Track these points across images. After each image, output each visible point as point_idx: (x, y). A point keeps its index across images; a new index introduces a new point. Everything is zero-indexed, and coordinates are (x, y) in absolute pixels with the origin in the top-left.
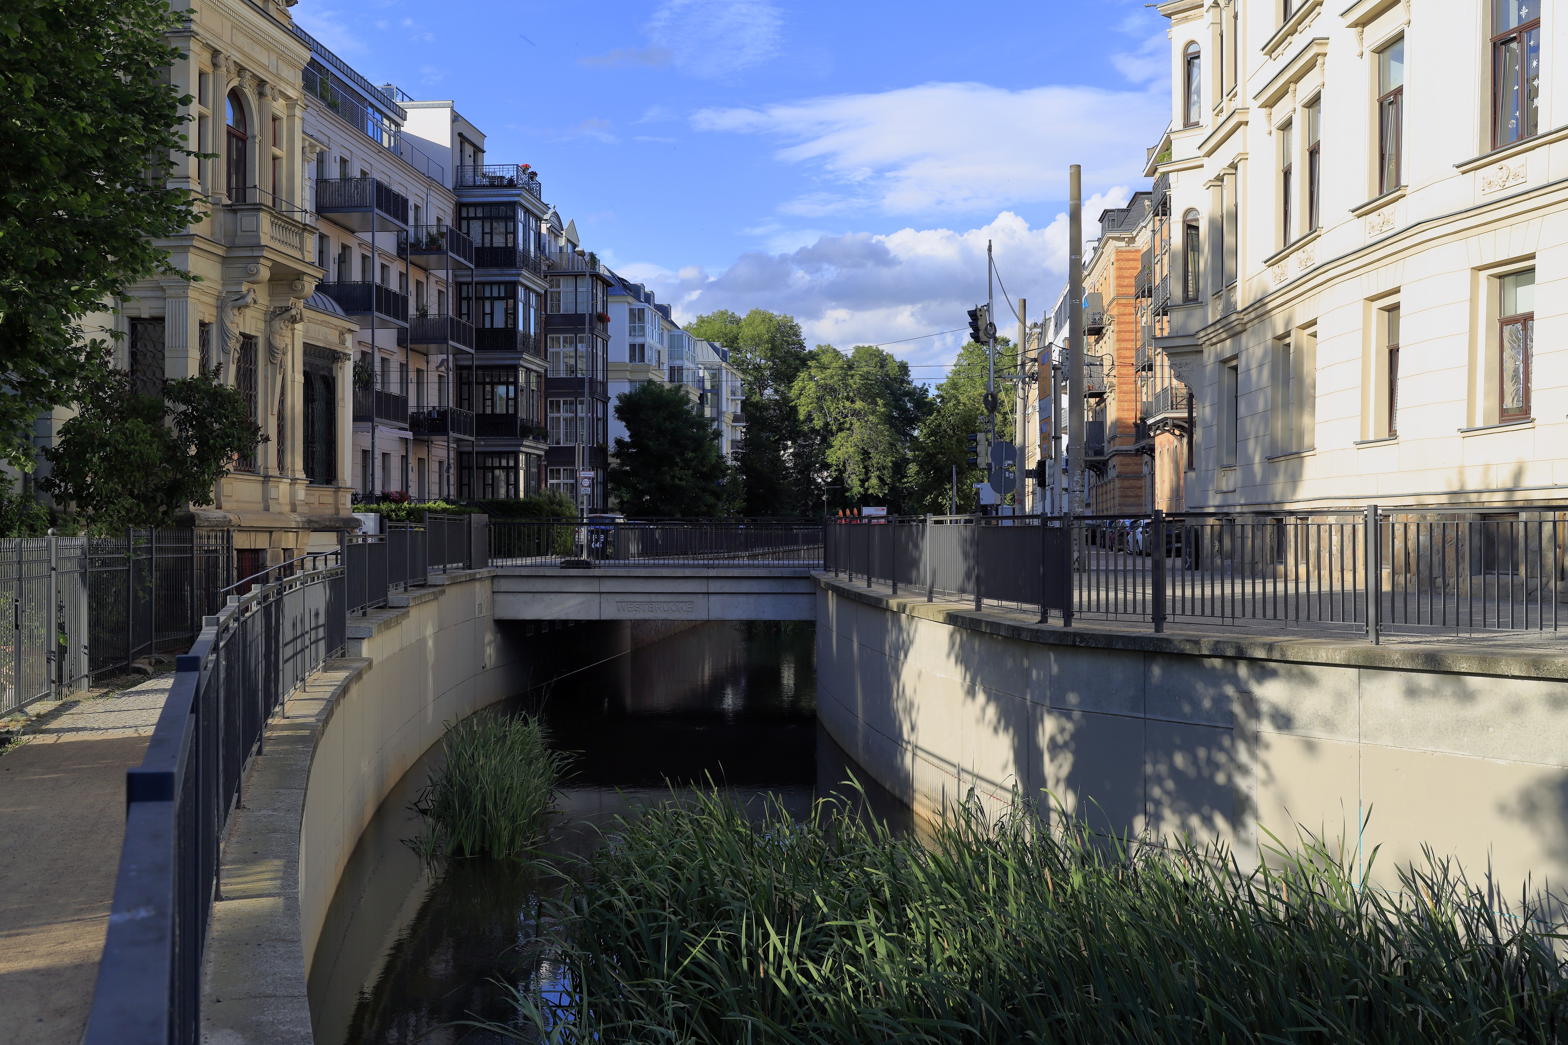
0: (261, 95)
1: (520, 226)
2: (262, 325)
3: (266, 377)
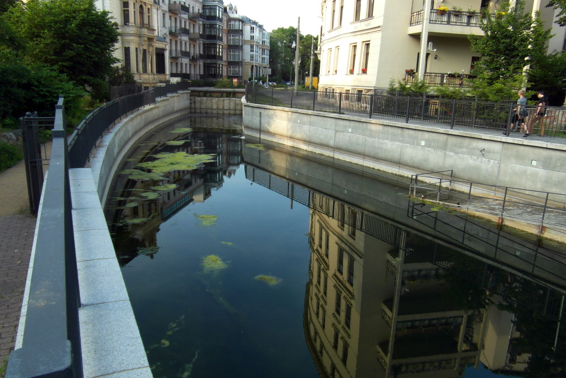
0: (146, 5)
1: (217, 11)
2: (147, 47)
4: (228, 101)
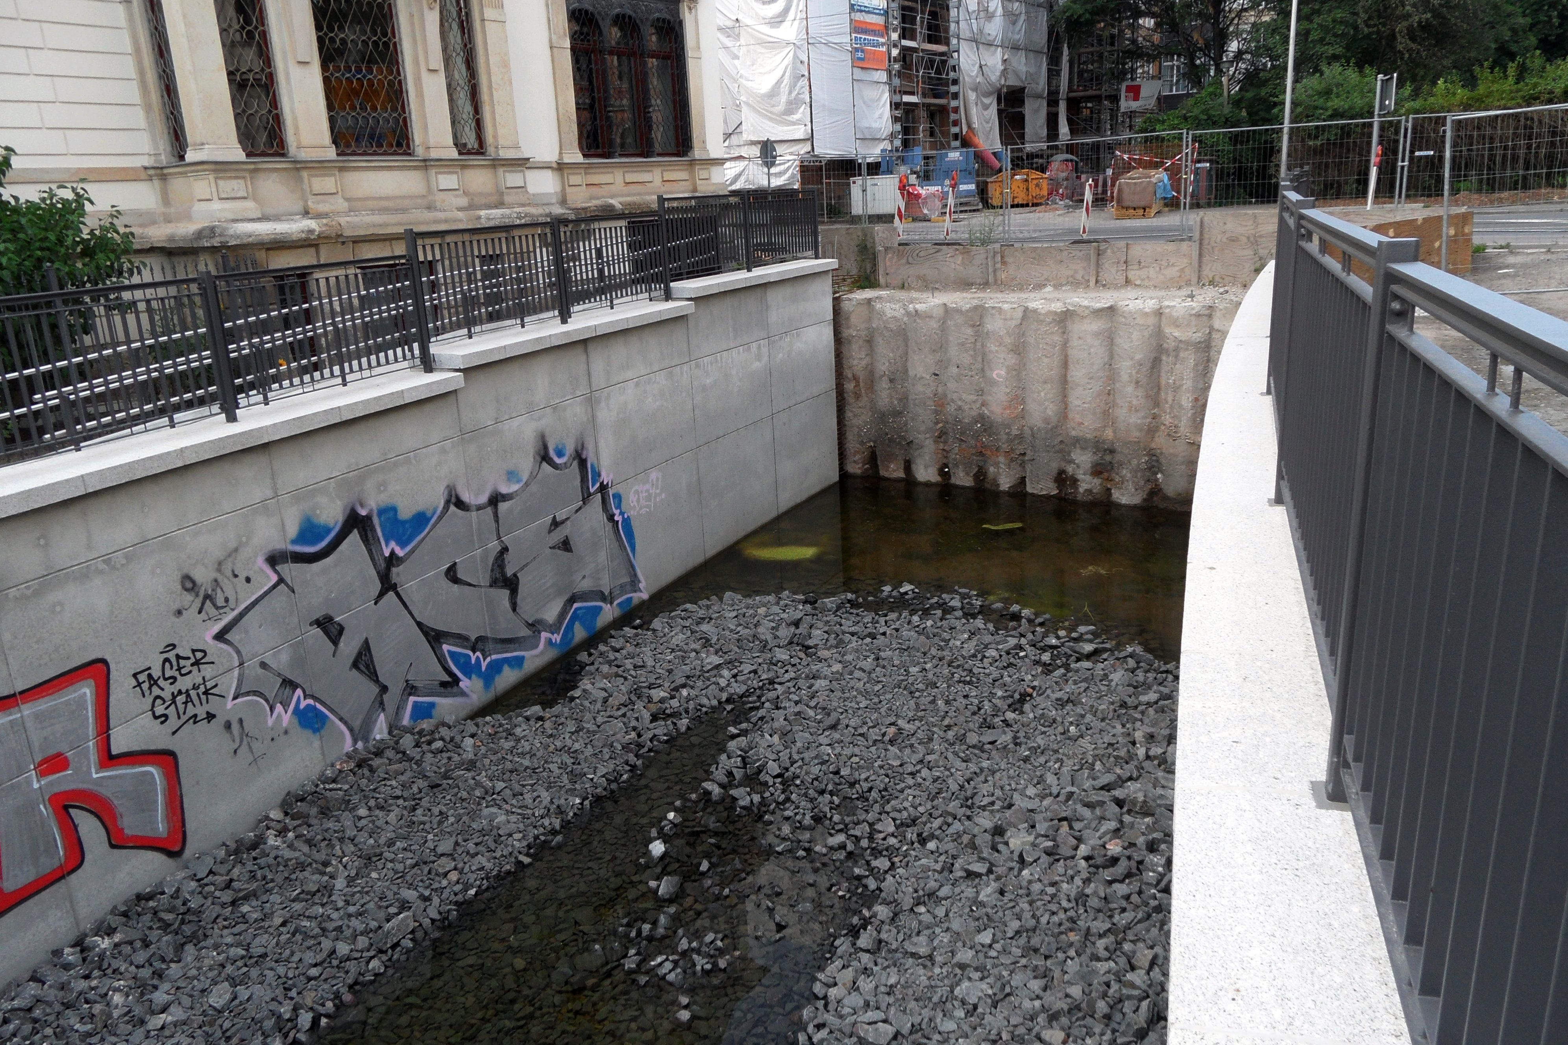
4: (1095, 326)
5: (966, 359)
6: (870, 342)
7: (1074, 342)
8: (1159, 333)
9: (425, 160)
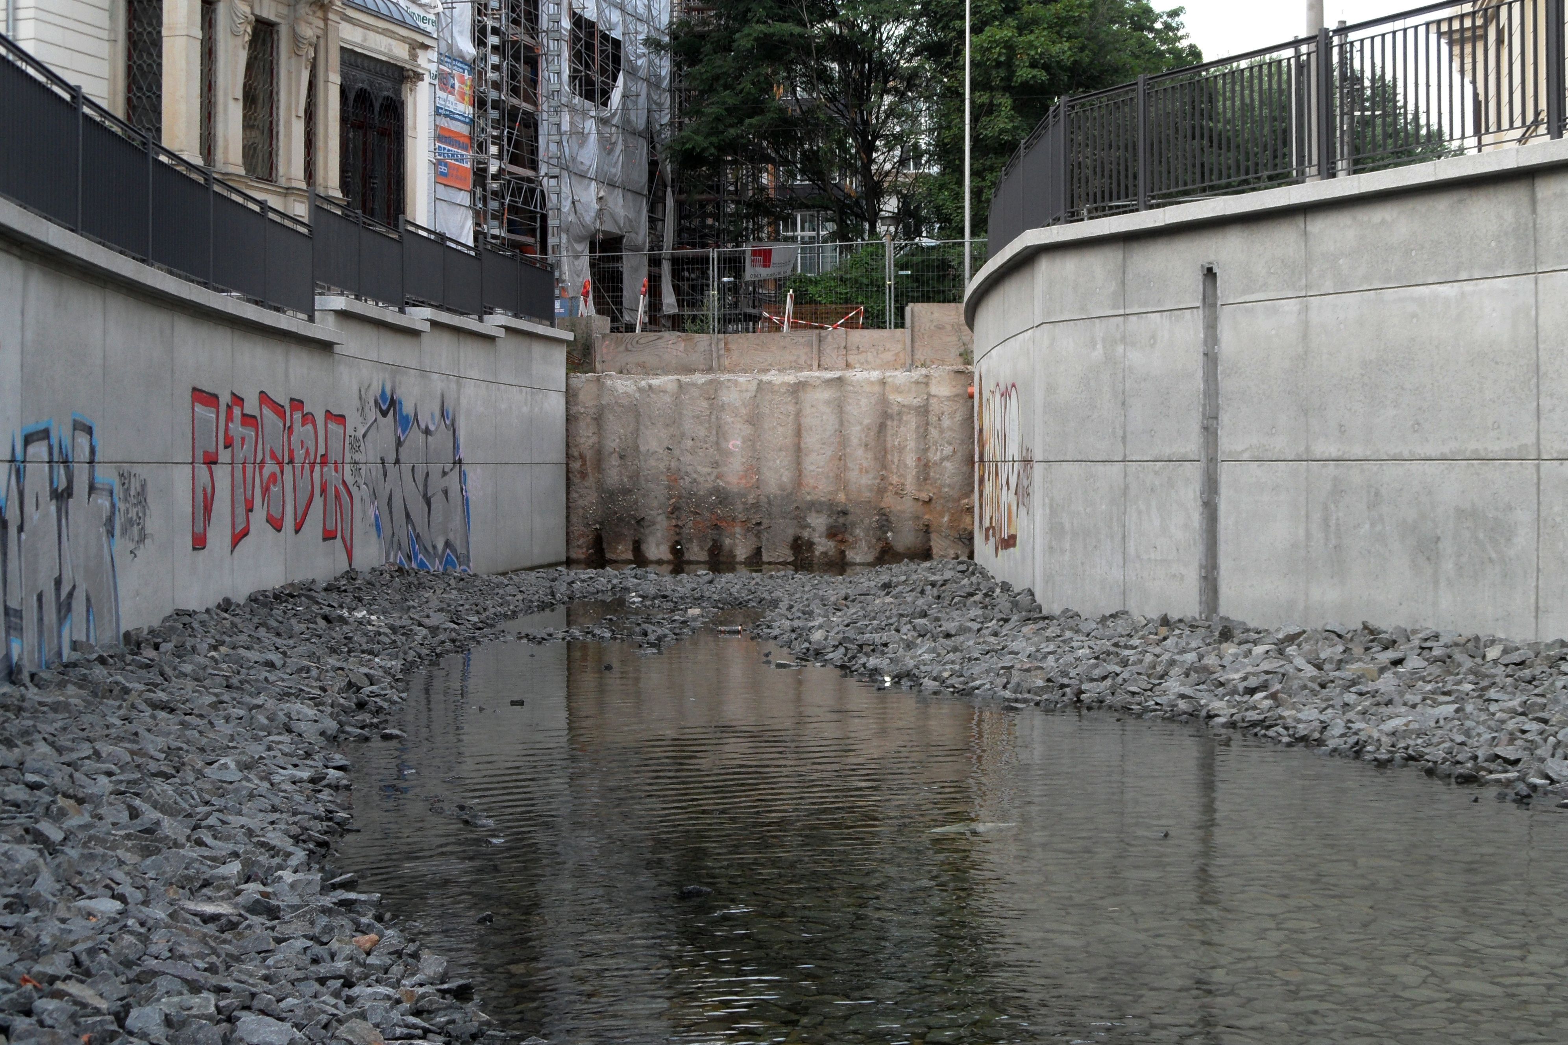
2: (284, 10)
3: (290, 72)
4: (825, 394)
5: (702, 432)
6: (598, 419)
7: (807, 411)
8: (884, 400)
9: (287, 189)
